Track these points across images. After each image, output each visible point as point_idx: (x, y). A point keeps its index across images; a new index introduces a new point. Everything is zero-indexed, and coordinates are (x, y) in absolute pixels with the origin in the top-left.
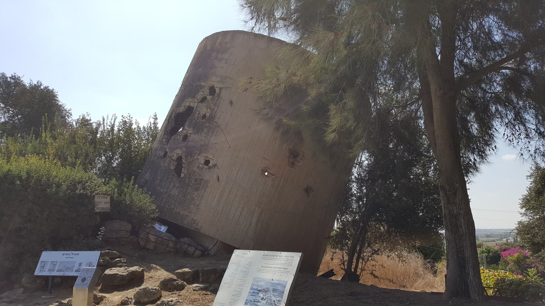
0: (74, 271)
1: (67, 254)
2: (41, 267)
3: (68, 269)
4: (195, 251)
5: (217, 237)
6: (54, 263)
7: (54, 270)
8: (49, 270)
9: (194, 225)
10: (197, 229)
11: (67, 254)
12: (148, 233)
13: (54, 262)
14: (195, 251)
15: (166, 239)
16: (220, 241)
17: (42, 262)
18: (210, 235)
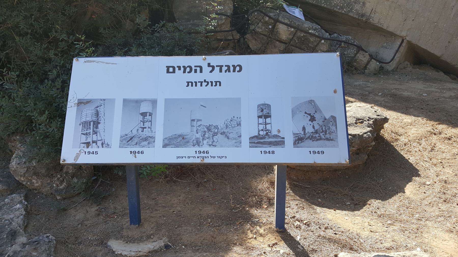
0: (245, 141)
1: (187, 69)
2: (85, 124)
3: (211, 133)
4: (368, 62)
5: (403, 34)
6: (141, 111)
7: (149, 140)
8: (127, 140)
9: (357, 7)
10: (363, 15)
11: (187, 69)
12: (277, 21)
13: (138, 102)
14: (368, 62)
15: (313, 35)
16: (409, 43)
17: (81, 103)
18: (390, 29)
